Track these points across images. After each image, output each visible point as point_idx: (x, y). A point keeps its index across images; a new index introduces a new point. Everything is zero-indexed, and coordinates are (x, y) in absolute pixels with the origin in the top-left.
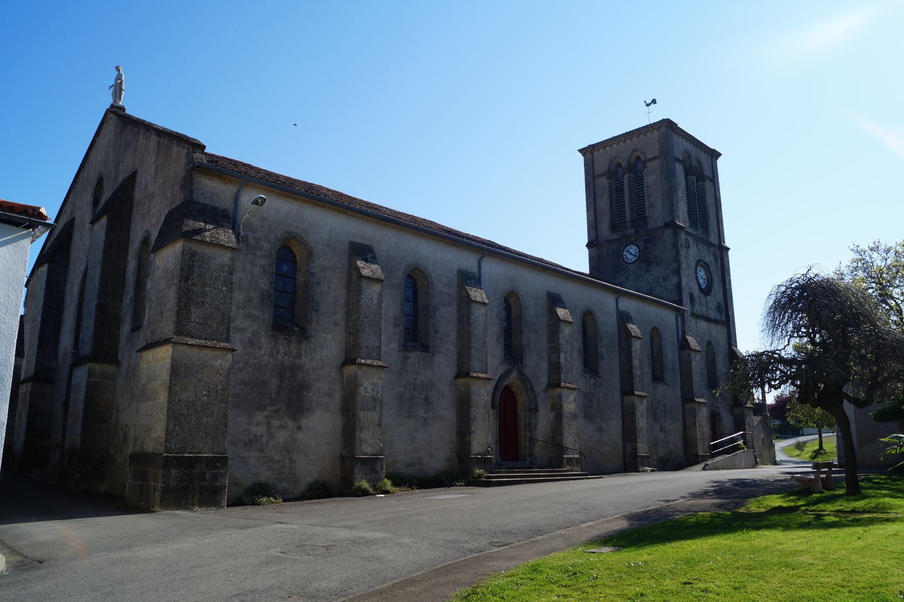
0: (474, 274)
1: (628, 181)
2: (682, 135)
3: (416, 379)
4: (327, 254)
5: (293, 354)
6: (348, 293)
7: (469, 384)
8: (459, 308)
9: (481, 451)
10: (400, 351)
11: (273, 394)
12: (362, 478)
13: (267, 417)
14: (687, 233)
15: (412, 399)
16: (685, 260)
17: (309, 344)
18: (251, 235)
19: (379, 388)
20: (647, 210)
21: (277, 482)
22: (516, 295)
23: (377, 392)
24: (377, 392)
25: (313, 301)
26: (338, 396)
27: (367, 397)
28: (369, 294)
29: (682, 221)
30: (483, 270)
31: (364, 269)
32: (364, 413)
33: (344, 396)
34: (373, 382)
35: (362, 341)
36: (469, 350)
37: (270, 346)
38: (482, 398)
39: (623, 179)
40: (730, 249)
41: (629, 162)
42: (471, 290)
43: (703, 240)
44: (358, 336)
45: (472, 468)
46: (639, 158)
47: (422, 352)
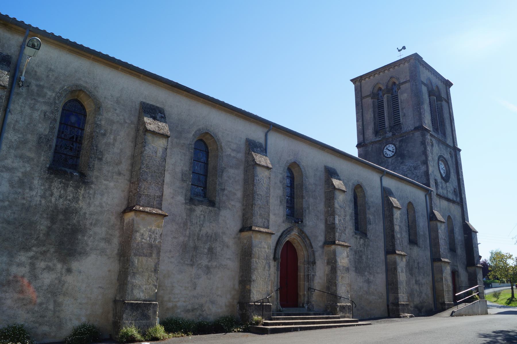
0: (260, 144)
1: (387, 99)
2: (426, 67)
3: (200, 230)
4: (116, 110)
5: (68, 198)
6: (135, 146)
7: (251, 237)
8: (246, 171)
9: (261, 299)
10: (186, 203)
11: (41, 235)
12: (131, 323)
13: (31, 258)
14: (431, 135)
15: (195, 248)
16: (430, 154)
17: (88, 189)
18: (35, 82)
19: (157, 235)
20: (401, 119)
21: (37, 325)
22: (298, 166)
23: (155, 239)
24: (155, 239)
25: (97, 150)
26: (116, 241)
27: (143, 244)
28: (154, 147)
29: (427, 124)
30: (269, 142)
31: (150, 124)
32: (138, 259)
33: (123, 242)
34: (151, 229)
35: (142, 189)
36: (252, 207)
37: (42, 188)
38: (263, 250)
39: (383, 98)
40: (461, 150)
41: (387, 86)
42: (256, 155)
43: (443, 142)
44: (139, 184)
45: (251, 314)
46: (394, 83)
47: (208, 206)
